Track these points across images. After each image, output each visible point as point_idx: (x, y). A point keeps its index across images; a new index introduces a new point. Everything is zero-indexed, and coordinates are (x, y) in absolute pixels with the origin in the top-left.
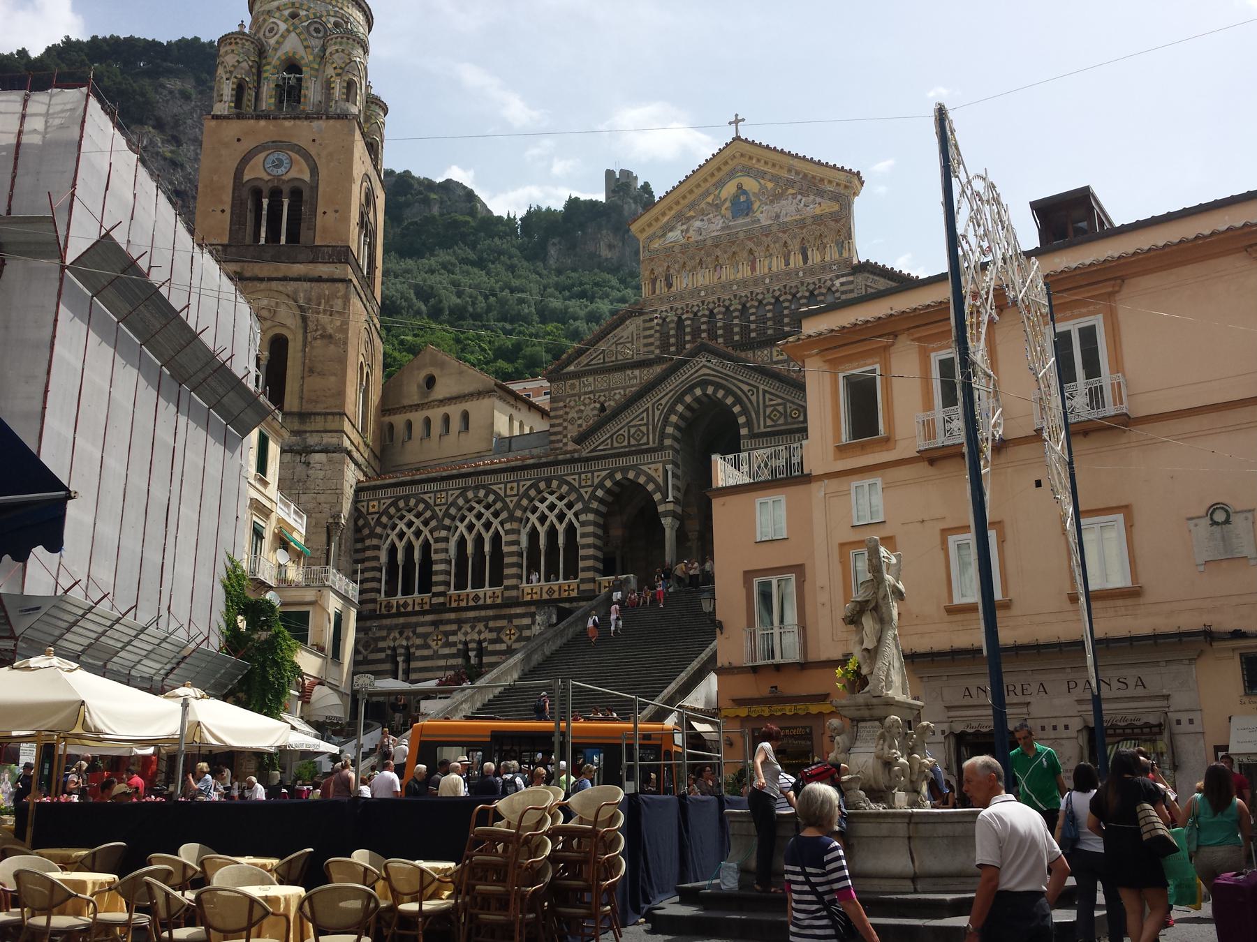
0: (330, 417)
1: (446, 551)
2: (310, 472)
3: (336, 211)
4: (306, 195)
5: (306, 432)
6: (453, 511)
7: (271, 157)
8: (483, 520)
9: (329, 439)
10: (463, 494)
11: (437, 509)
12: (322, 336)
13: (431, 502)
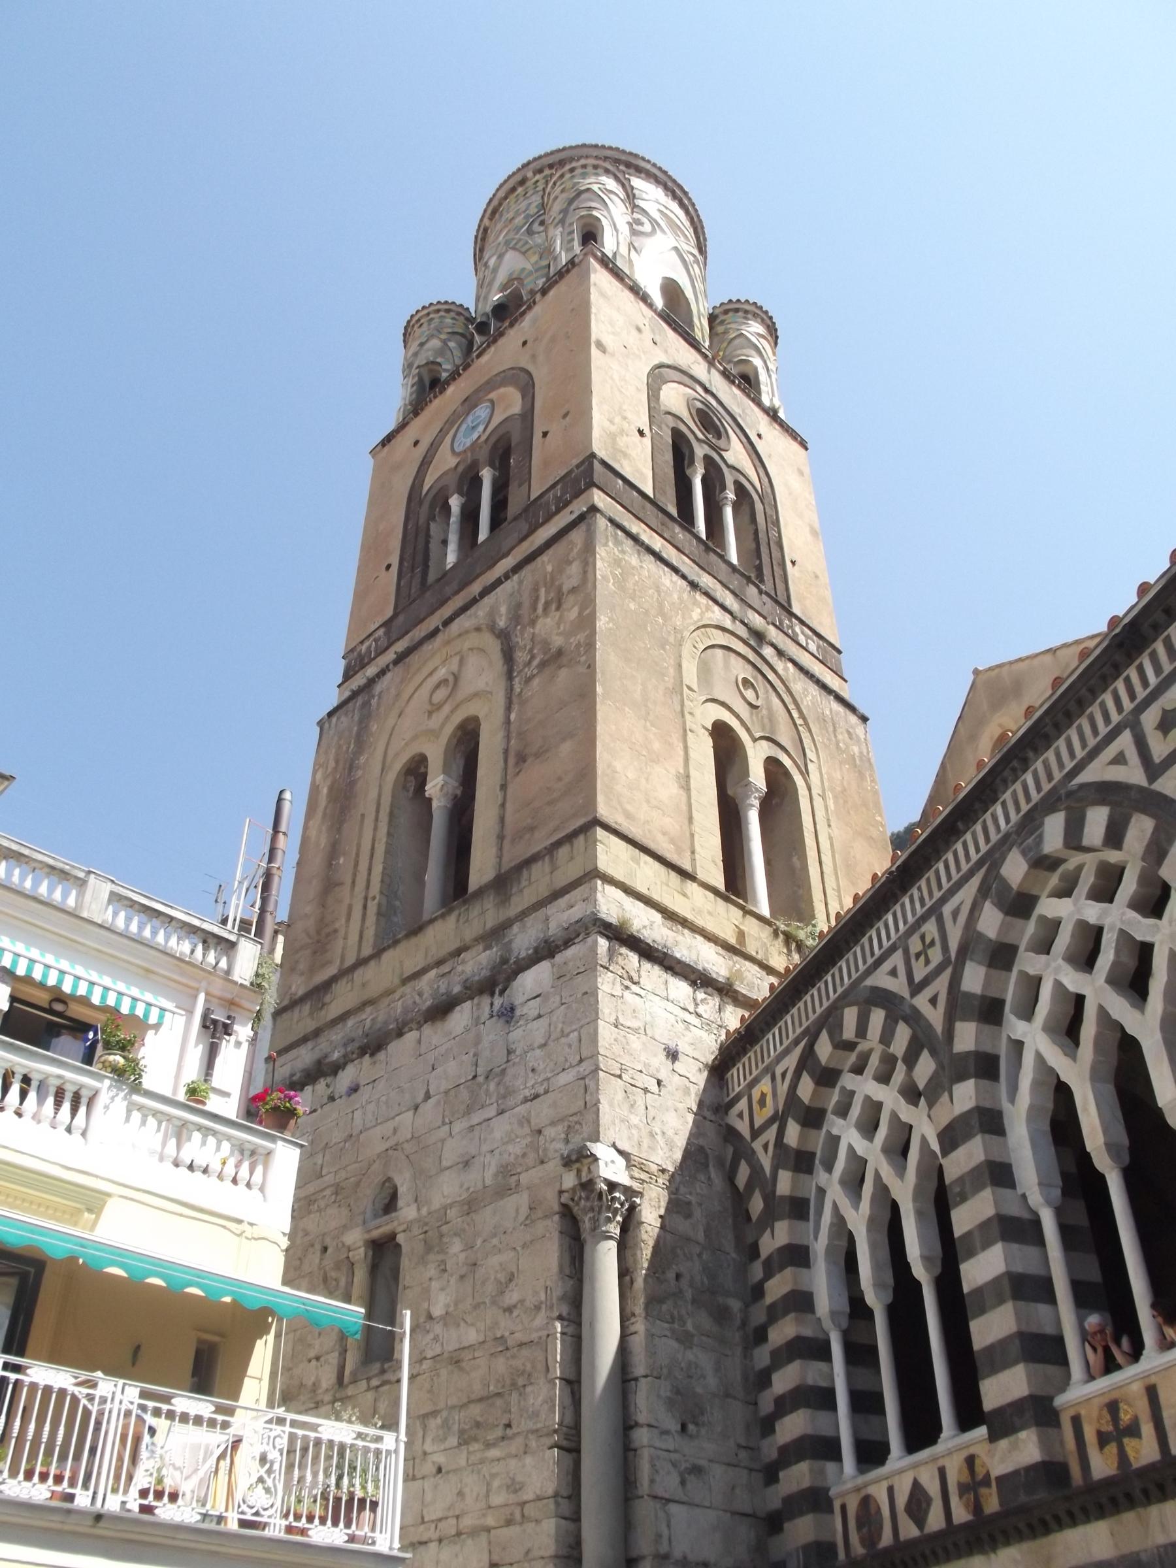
0: (563, 852)
1: (999, 1174)
2: (517, 1034)
3: (565, 416)
4: (515, 439)
5: (506, 925)
6: (974, 979)
7: (464, 427)
8: (1106, 958)
9: (561, 916)
10: (992, 887)
11: (921, 1002)
12: (543, 665)
13: (898, 986)
